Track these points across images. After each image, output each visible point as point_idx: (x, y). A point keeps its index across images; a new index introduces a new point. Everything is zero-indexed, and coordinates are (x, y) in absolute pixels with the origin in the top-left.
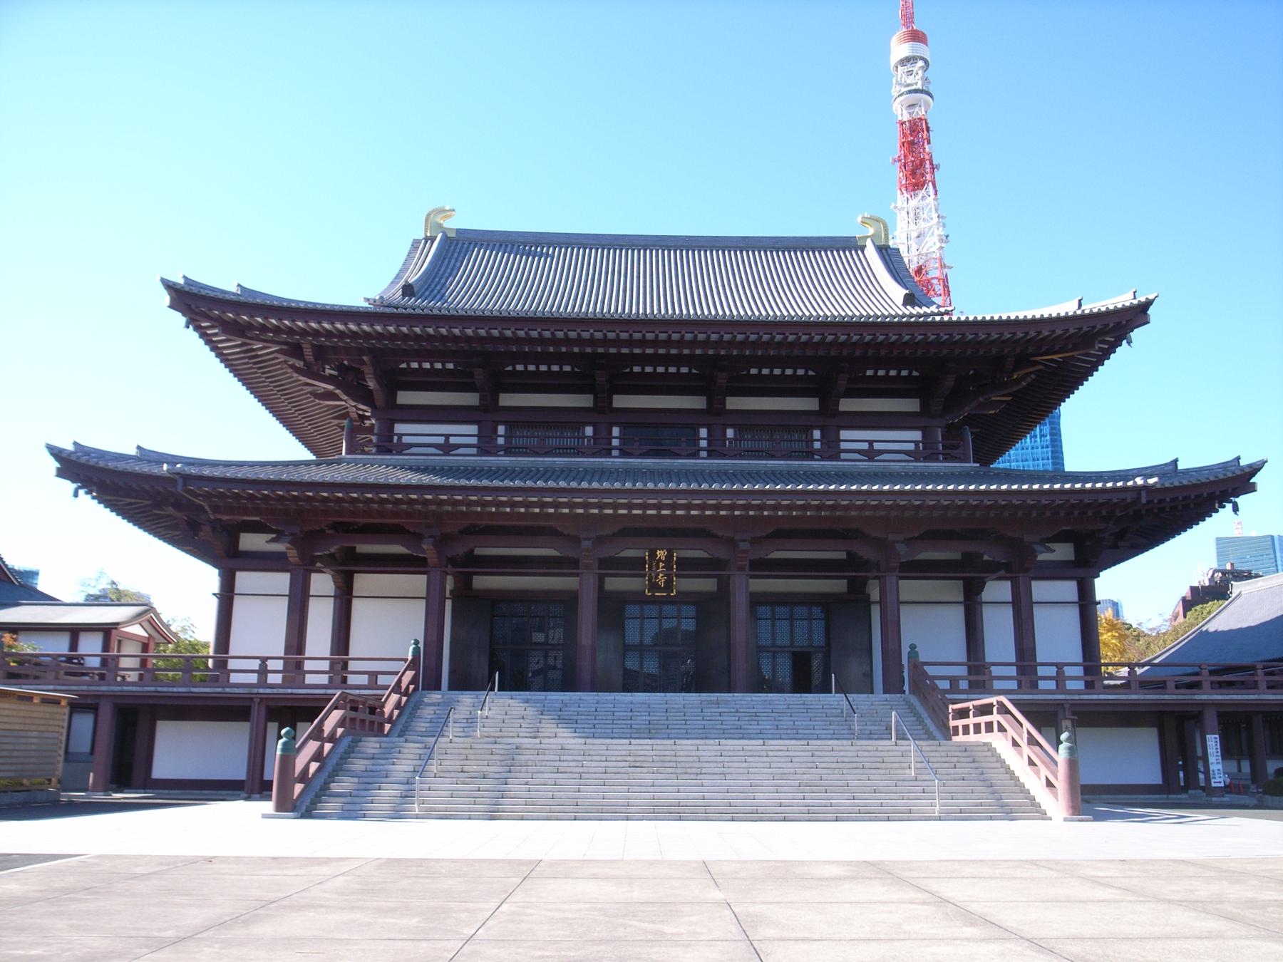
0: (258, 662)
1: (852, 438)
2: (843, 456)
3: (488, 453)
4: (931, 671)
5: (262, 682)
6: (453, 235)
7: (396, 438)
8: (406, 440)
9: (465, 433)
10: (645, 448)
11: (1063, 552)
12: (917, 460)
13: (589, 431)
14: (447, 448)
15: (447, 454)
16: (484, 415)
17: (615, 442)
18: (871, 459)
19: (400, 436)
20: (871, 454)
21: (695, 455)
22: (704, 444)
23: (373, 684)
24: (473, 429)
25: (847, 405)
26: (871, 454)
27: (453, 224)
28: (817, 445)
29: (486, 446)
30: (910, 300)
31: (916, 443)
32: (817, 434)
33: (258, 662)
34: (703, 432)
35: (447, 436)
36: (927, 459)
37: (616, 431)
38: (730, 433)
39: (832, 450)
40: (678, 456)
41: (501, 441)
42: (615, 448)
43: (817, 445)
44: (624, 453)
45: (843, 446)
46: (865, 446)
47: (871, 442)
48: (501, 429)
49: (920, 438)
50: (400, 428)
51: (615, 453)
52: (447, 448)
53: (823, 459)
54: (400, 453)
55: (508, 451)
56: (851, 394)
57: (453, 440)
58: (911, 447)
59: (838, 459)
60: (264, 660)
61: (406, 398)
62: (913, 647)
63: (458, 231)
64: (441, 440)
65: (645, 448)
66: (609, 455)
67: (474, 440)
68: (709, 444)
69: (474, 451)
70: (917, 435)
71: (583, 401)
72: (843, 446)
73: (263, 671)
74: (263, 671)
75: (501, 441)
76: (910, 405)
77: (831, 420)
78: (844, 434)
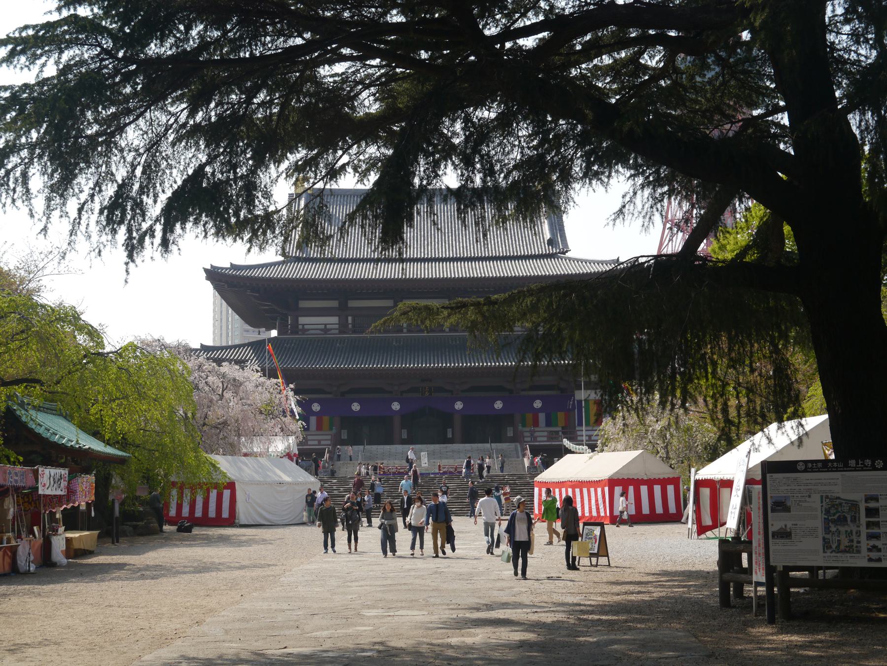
3: (345, 333)
7: (300, 327)
15: (326, 334)
16: (342, 311)
19: (303, 325)
24: (334, 320)
29: (343, 327)
30: (551, 242)
35: (325, 325)
41: (350, 326)
48: (350, 319)
50: (303, 320)
51: (405, 330)
52: (326, 330)
54: (303, 334)
57: (328, 326)
61: (304, 304)
64: (323, 327)
67: (337, 326)
75: (350, 326)
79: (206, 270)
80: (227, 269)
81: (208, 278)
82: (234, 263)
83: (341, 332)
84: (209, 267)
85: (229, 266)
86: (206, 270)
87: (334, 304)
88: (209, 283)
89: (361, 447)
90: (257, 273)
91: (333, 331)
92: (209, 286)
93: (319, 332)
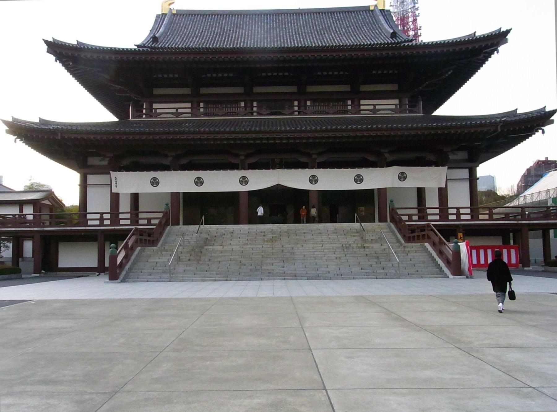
0: (99, 215)
1: (366, 104)
2: (362, 112)
4: (399, 212)
5: (102, 224)
8: (158, 111)
9: (185, 108)
10: (269, 112)
11: (462, 155)
12: (396, 113)
13: (243, 104)
14: (177, 114)
16: (194, 99)
17: (255, 109)
18: (375, 113)
19: (156, 109)
20: (374, 111)
21: (292, 114)
22: (296, 108)
23: (149, 223)
25: (364, 88)
26: (374, 111)
33: (99, 215)
34: (296, 103)
35: (177, 109)
36: (400, 113)
38: (308, 103)
39: (357, 109)
40: (284, 114)
41: (202, 110)
42: (255, 112)
43: (349, 107)
44: (259, 114)
45: (362, 107)
47: (374, 106)
49: (398, 103)
50: (155, 106)
51: (255, 114)
52: (177, 114)
53: (352, 114)
55: (206, 114)
56: (364, 83)
57: (180, 110)
58: (393, 107)
59: (359, 113)
60: (102, 214)
61: (158, 91)
62: (392, 201)
65: (269, 112)
66: (252, 114)
67: (189, 110)
68: (298, 109)
69: (190, 115)
70: (396, 101)
71: (239, 90)
72: (362, 107)
73: (102, 220)
74: (102, 220)
76: (393, 87)
77: (357, 96)
78: (362, 102)
82: (80, 40)
83: (193, 114)
85: (76, 43)
87: (187, 91)
89: (197, 227)
91: (183, 115)
93: (172, 116)
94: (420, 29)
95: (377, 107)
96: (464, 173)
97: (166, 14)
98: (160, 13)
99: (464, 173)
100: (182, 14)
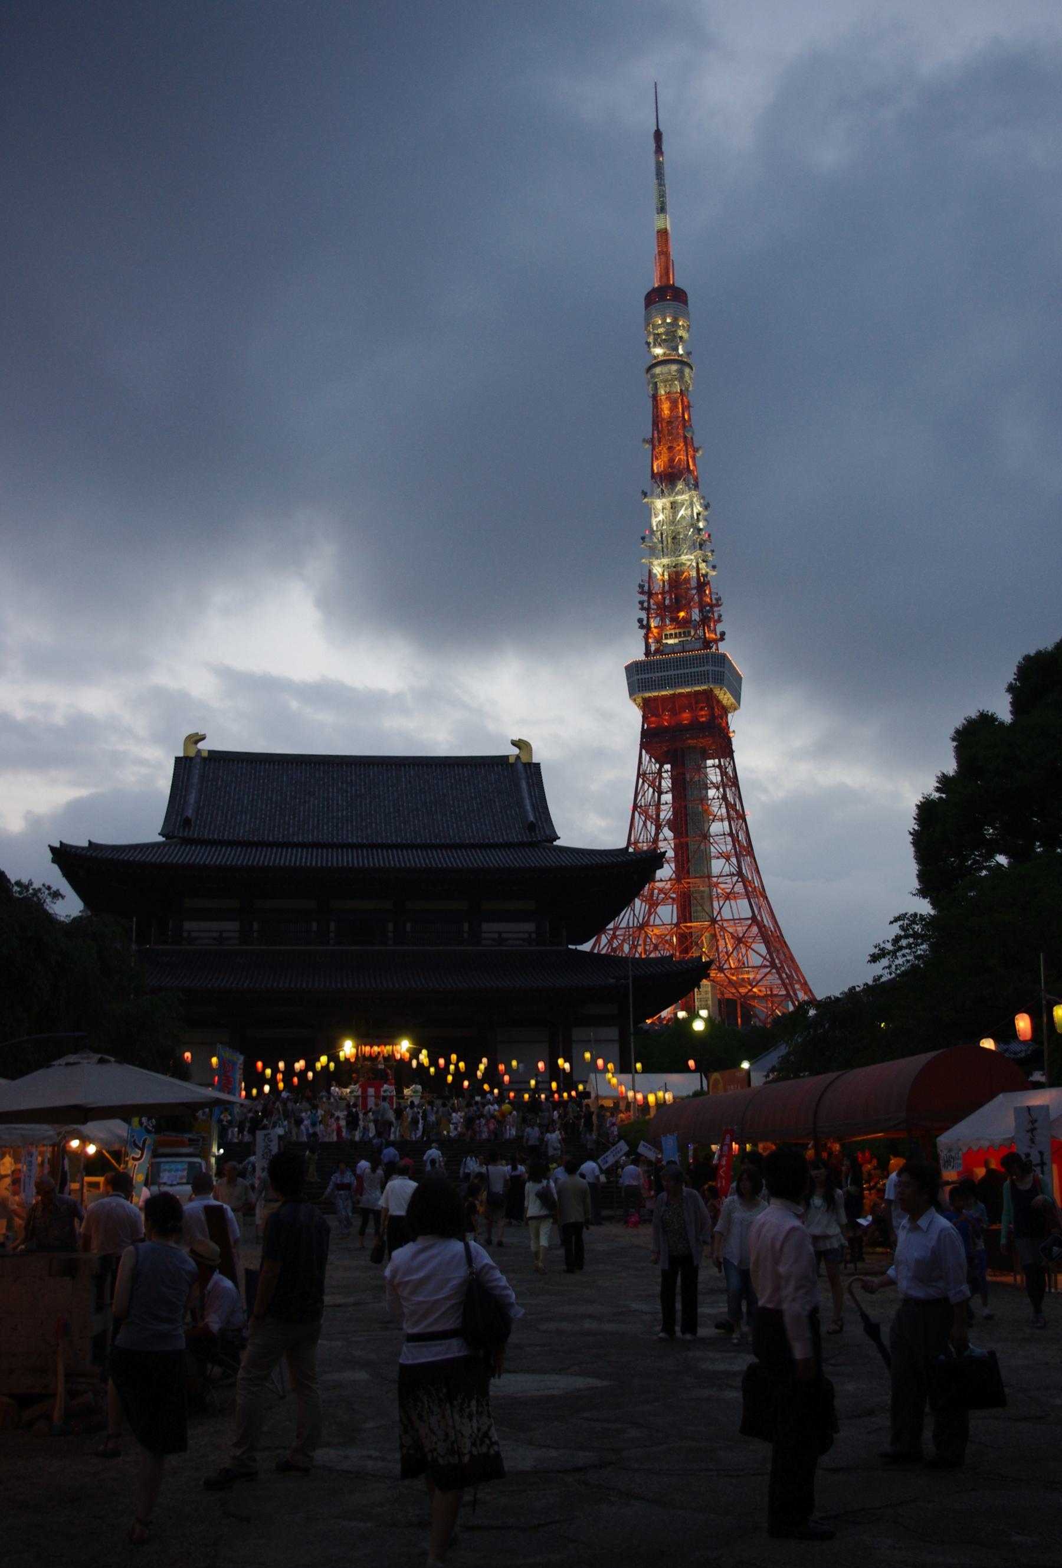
1: (491, 929)
6: (205, 754)
7: (185, 934)
8: (193, 934)
17: (332, 935)
22: (390, 935)
24: (235, 926)
27: (204, 746)
28: (466, 935)
31: (530, 933)
32: (466, 927)
34: (391, 926)
37: (332, 926)
38: (408, 926)
41: (256, 934)
43: (466, 935)
46: (496, 936)
47: (500, 933)
50: (188, 925)
57: (225, 935)
58: (526, 935)
63: (210, 752)
70: (531, 927)
78: (486, 926)
79: (52, 849)
80: (83, 848)
81: (54, 861)
84: (58, 845)
85: (86, 844)
86: (52, 849)
88: (55, 867)
90: (125, 856)
92: (55, 868)
94: (718, 605)
95: (504, 935)
96: (613, 1033)
97: (191, 759)
98: (181, 754)
99: (613, 1033)
100: (216, 756)
